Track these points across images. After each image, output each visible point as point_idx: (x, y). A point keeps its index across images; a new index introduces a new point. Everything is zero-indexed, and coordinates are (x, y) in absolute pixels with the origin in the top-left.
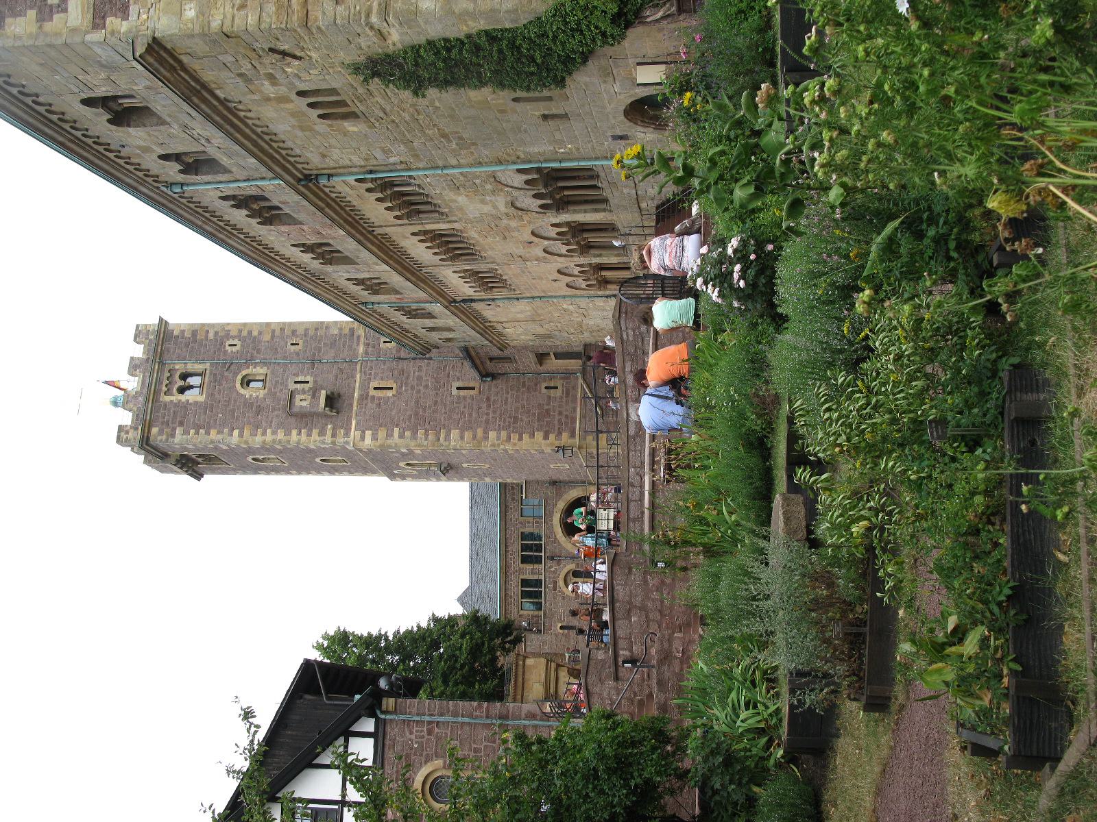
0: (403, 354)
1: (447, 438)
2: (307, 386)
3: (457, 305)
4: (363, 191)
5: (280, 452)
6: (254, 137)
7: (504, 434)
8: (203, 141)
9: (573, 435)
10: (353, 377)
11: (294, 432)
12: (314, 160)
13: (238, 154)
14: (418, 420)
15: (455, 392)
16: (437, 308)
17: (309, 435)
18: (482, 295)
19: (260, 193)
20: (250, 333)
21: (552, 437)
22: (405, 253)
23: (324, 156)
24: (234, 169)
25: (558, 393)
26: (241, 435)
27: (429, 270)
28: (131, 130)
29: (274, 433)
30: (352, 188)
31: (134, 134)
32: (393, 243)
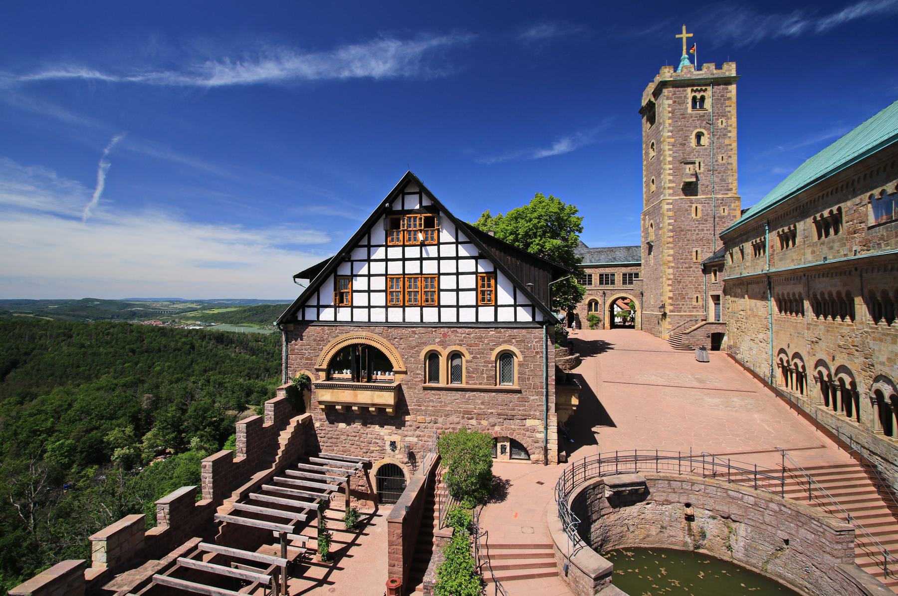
0: (717, 219)
1: (669, 248)
2: (697, 169)
5: (658, 159)
7: (672, 277)
9: (671, 311)
10: (703, 194)
11: (671, 166)
14: (678, 232)
15: (694, 250)
17: (669, 174)
20: (730, 132)
21: (670, 301)
25: (694, 303)
26: (669, 137)
29: (670, 156)
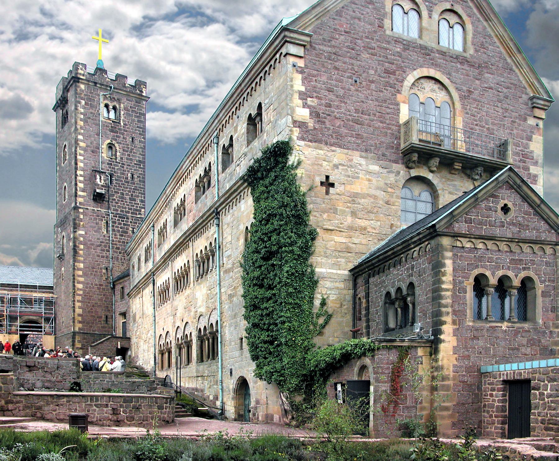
3: (151, 276)
4: (210, 240)
6: (239, 191)
8: (238, 162)
12: (227, 219)
13: (231, 179)
16: (150, 265)
18: (156, 290)
19: (212, 185)
22: (179, 255)
23: (228, 224)
24: (223, 174)
27: (170, 265)
28: (246, 124)
30: (213, 235)
31: (244, 126)
32: (184, 250)
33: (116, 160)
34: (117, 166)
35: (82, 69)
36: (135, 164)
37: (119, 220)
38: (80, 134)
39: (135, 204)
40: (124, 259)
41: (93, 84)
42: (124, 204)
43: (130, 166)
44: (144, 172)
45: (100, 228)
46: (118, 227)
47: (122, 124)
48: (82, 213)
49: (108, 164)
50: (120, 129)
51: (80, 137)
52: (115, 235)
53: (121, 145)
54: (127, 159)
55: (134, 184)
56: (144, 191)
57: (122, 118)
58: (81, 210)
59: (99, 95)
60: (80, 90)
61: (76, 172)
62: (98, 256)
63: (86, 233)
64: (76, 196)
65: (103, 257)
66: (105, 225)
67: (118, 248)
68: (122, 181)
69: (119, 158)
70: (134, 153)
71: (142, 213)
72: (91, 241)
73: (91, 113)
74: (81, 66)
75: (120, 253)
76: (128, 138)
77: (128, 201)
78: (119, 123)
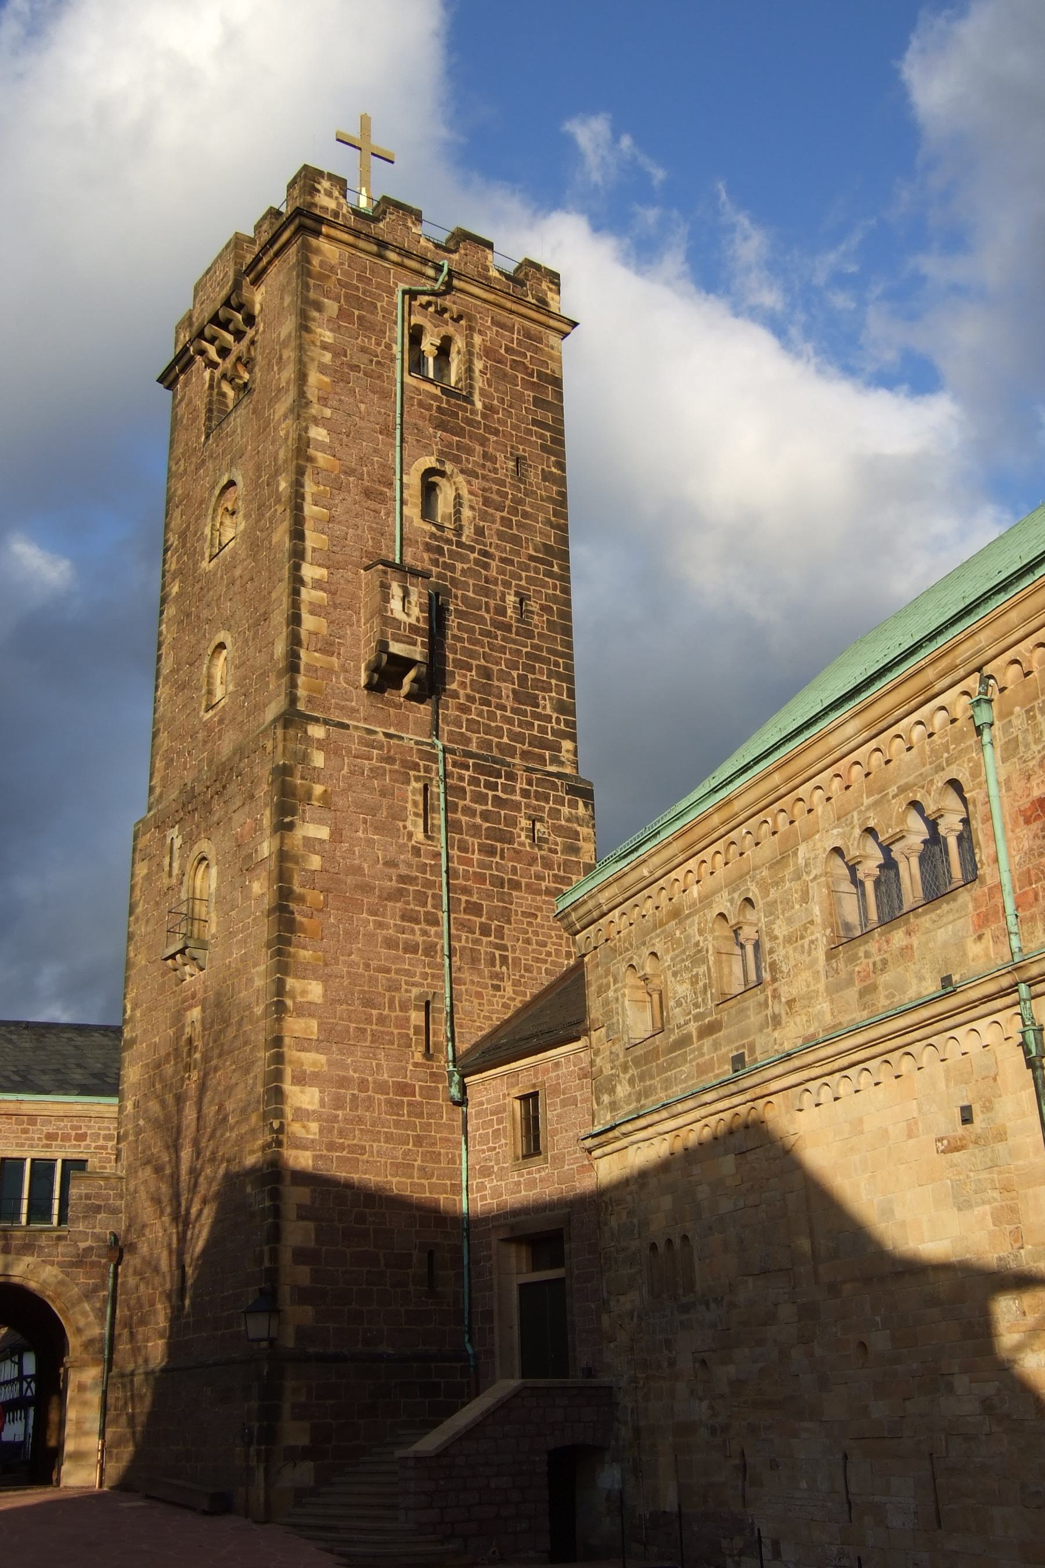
33: (460, 535)
34: (464, 559)
35: (329, 194)
36: (531, 558)
37: (474, 782)
38: (316, 421)
39: (537, 716)
40: (504, 960)
41: (374, 248)
42: (492, 716)
43: (511, 562)
44: (566, 591)
45: (398, 815)
46: (472, 813)
47: (479, 405)
48: (321, 745)
49: (428, 548)
50: (470, 422)
51: (318, 433)
52: (463, 848)
53: (475, 482)
54: (501, 535)
55: (530, 635)
56: (569, 668)
57: (479, 383)
58: (317, 732)
59: (391, 292)
60: (322, 264)
61: (297, 567)
62: (390, 943)
63: (337, 835)
64: (293, 666)
65: (411, 948)
66: (420, 799)
67: (475, 909)
68: (481, 620)
69: (468, 532)
70: (525, 515)
71: (565, 756)
72: (358, 870)
73: (363, 350)
74: (326, 184)
75: (485, 931)
76: (500, 456)
77: (509, 704)
78: (468, 399)
